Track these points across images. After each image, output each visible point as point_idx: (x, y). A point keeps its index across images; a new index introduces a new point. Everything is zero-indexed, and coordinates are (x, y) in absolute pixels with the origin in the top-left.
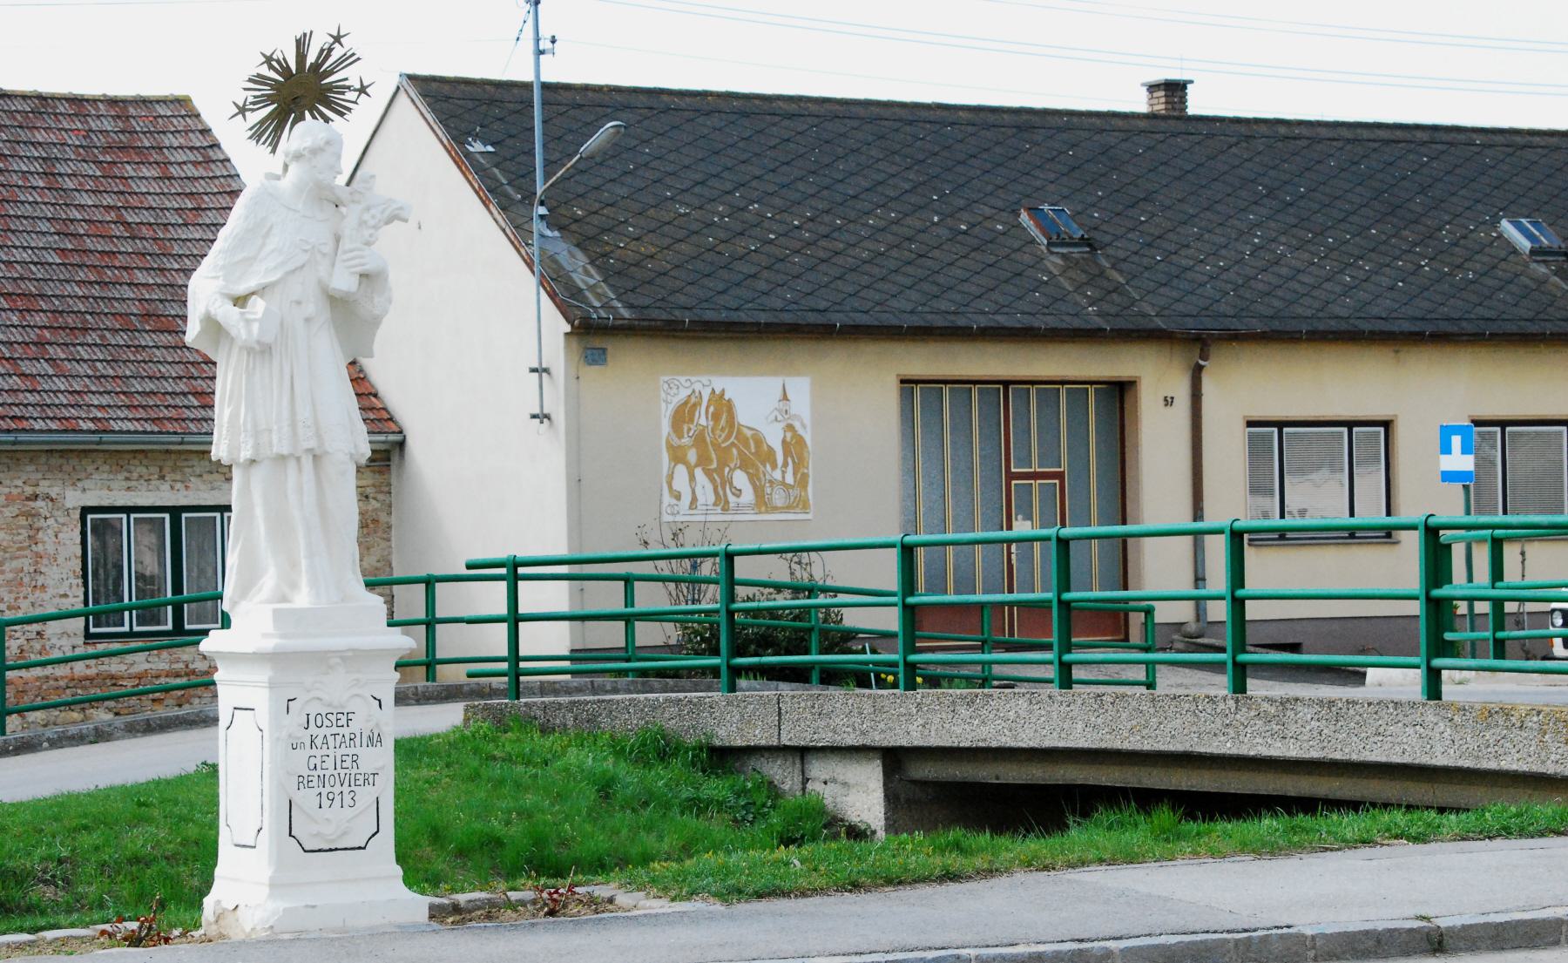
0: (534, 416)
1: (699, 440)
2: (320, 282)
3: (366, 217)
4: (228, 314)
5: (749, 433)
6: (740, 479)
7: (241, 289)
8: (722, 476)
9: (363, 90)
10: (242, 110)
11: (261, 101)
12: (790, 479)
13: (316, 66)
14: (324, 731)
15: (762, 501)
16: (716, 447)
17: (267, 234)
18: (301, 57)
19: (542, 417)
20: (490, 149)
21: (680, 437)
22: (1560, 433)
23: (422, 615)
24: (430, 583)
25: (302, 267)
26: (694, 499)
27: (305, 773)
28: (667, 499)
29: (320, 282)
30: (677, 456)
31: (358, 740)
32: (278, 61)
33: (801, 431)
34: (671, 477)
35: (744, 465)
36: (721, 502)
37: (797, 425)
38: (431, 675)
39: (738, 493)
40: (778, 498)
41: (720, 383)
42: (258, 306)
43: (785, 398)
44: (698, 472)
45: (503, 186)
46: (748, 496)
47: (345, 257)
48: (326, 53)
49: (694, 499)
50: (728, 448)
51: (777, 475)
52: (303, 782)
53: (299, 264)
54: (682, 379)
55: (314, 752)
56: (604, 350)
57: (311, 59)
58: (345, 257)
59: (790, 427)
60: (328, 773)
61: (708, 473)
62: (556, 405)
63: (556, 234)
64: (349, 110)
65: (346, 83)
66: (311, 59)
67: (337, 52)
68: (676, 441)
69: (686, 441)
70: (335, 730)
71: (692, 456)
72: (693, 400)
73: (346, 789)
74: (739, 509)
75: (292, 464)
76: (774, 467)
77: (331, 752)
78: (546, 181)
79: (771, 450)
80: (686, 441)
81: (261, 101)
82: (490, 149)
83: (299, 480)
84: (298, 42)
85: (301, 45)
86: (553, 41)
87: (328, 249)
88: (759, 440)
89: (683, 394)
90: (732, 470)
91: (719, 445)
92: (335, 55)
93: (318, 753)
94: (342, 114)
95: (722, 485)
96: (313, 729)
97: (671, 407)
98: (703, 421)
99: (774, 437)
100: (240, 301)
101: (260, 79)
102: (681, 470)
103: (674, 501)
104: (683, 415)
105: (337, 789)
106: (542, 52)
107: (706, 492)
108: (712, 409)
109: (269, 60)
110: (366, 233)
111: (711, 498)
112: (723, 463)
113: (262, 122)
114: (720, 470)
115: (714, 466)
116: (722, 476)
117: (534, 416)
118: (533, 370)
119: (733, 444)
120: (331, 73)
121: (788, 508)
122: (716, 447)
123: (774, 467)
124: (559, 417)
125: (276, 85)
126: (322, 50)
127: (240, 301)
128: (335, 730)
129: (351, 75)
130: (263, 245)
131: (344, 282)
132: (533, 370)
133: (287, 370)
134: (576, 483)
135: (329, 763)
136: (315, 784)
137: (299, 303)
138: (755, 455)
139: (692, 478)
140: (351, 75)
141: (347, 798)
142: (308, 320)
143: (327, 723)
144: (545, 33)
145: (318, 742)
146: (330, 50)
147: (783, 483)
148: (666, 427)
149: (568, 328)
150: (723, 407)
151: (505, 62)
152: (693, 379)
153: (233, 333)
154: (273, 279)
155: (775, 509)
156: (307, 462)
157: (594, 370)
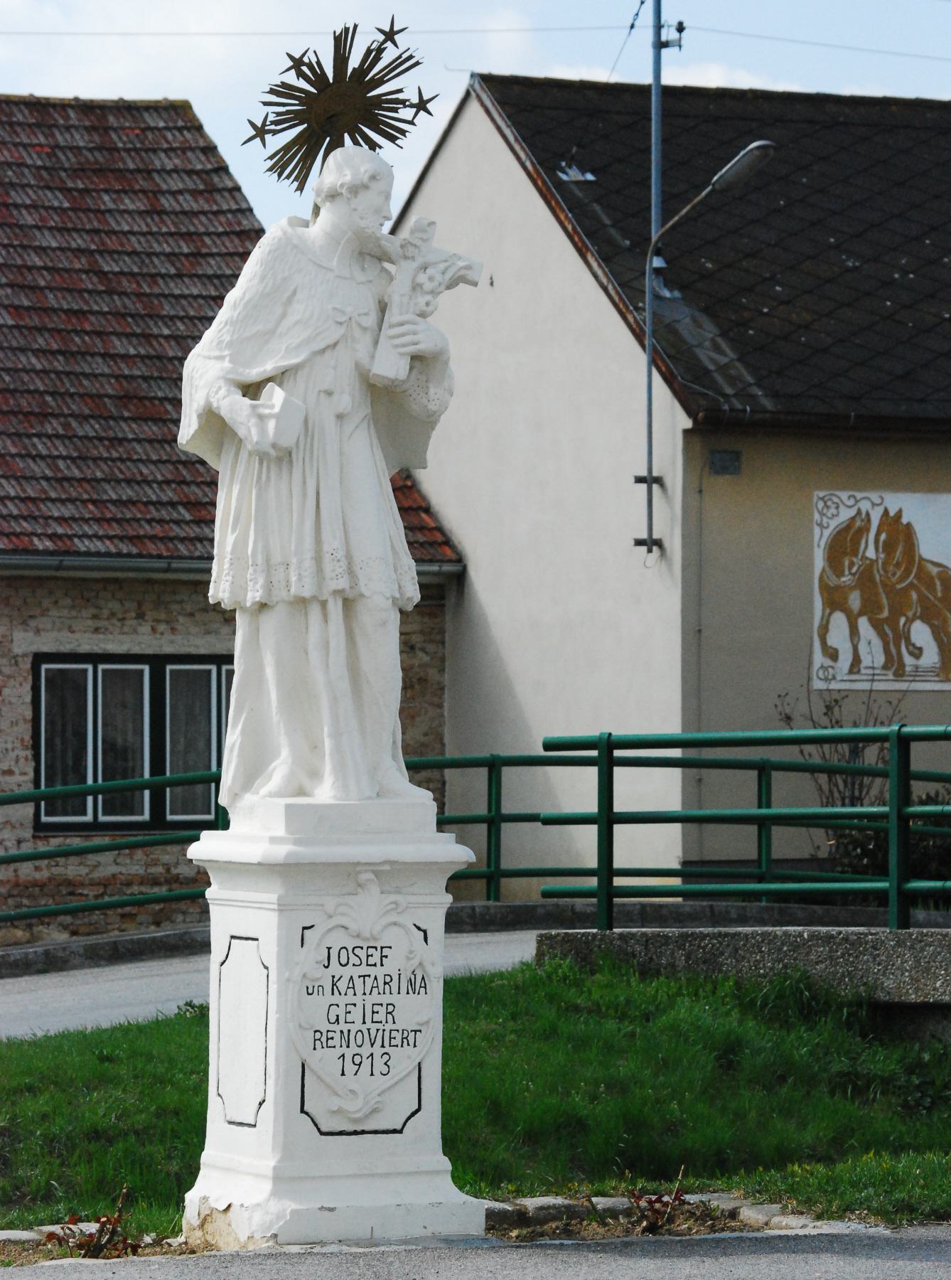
0: (639, 543)
1: (865, 579)
2: (357, 366)
3: (422, 278)
4: (234, 407)
7: (254, 373)
8: (895, 629)
9: (422, 106)
10: (260, 132)
11: (285, 121)
13: (361, 71)
14: (348, 972)
16: (890, 590)
17: (289, 301)
18: (341, 58)
19: (651, 543)
20: (590, 177)
21: (840, 574)
23: (482, 810)
24: (495, 766)
25: (335, 345)
26: (856, 660)
27: (324, 1027)
28: (819, 658)
29: (357, 366)
30: (834, 600)
31: (394, 985)
32: (310, 66)
34: (824, 629)
36: (893, 664)
38: (493, 890)
39: (917, 652)
41: (896, 501)
42: (275, 396)
44: (863, 623)
45: (603, 225)
48: (374, 54)
49: (856, 660)
50: (905, 590)
52: (321, 1039)
53: (331, 341)
54: (844, 495)
55: (336, 999)
56: (737, 455)
57: (354, 62)
60: (354, 1028)
61: (876, 625)
62: (670, 527)
63: (677, 294)
64: (403, 132)
65: (400, 96)
66: (354, 62)
67: (390, 54)
68: (833, 581)
70: (364, 970)
71: (855, 601)
72: (858, 523)
73: (377, 1050)
74: (917, 673)
75: (315, 612)
77: (358, 1000)
78: (664, 223)
81: (285, 121)
82: (590, 177)
83: (324, 632)
84: (337, 39)
85: (342, 42)
86: (680, 28)
87: (370, 321)
89: (846, 514)
90: (910, 621)
92: (390, 54)
93: (342, 1000)
94: (392, 139)
95: (895, 638)
96: (335, 968)
97: (827, 533)
98: (871, 553)
100: (252, 390)
101: (283, 90)
102: (839, 621)
103: (828, 662)
104: (844, 544)
105: (366, 1050)
106: (666, 45)
107: (873, 653)
108: (883, 536)
109: (297, 64)
110: (422, 300)
111: (880, 659)
112: (896, 612)
113: (287, 148)
114: (892, 621)
115: (886, 614)
116: (895, 629)
117: (639, 543)
118: (639, 480)
119: (911, 585)
120: (380, 82)
122: (890, 590)
124: (675, 544)
125: (306, 98)
126: (369, 52)
127: (252, 390)
128: (364, 970)
129: (408, 85)
130: (284, 315)
131: (391, 366)
132: (639, 480)
135: (356, 1014)
136: (336, 1042)
137: (329, 393)
139: (854, 631)
140: (408, 85)
142: (340, 417)
143: (354, 960)
144: (670, 18)
145: (342, 985)
146: (380, 50)
148: (819, 562)
149: (688, 424)
150: (899, 534)
152: (859, 495)
153: (241, 432)
156: (335, 608)
157: (722, 481)
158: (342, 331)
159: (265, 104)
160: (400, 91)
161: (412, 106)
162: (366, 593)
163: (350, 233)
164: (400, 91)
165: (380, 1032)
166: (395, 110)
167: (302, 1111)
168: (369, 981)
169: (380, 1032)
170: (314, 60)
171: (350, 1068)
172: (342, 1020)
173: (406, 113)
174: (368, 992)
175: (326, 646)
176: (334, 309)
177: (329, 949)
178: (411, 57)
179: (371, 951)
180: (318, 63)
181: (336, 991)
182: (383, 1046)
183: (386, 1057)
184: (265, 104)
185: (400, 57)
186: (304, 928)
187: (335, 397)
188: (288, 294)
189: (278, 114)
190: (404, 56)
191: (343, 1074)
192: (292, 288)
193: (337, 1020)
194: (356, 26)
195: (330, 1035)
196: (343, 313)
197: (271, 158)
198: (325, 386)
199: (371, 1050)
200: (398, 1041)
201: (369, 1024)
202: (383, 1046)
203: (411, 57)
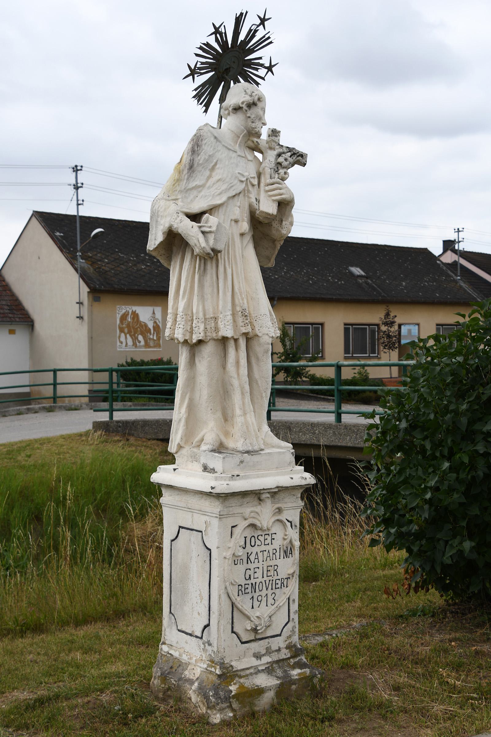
0: (77, 317)
1: (128, 326)
2: (250, 206)
3: (281, 159)
5: (143, 324)
6: (140, 338)
7: (195, 208)
8: (135, 336)
9: (270, 69)
10: (193, 72)
12: (155, 338)
13: (245, 42)
14: (256, 549)
15: (147, 345)
16: (133, 328)
17: (213, 169)
19: (81, 318)
20: (62, 234)
21: (123, 324)
22: (366, 328)
23: (52, 382)
24: (55, 371)
26: (127, 344)
28: (118, 344)
29: (250, 206)
30: (122, 330)
31: (278, 554)
32: (221, 34)
33: (158, 323)
34: (119, 337)
35: (142, 334)
36: (135, 345)
37: (157, 321)
38: (55, 402)
39: (140, 342)
40: (152, 344)
42: (211, 221)
43: (154, 313)
44: (128, 335)
45: (66, 246)
46: (143, 343)
47: (267, 188)
48: (252, 33)
49: (127, 344)
50: (137, 328)
51: (151, 337)
52: (242, 590)
54: (123, 307)
56: (99, 297)
57: (242, 37)
58: (267, 188)
59: (155, 322)
60: (258, 581)
61: (131, 336)
63: (84, 261)
65: (261, 61)
66: (242, 37)
68: (121, 326)
69: (124, 326)
70: (263, 548)
71: (126, 330)
73: (270, 592)
74: (140, 347)
75: (232, 343)
76: (150, 334)
79: (150, 329)
80: (124, 326)
82: (62, 234)
83: (236, 356)
86: (83, 201)
87: (255, 182)
88: (146, 325)
89: (124, 311)
90: (138, 335)
91: (134, 328)
95: (135, 339)
96: (249, 549)
97: (120, 315)
98: (129, 320)
99: (151, 325)
100: (195, 217)
102: (123, 335)
104: (124, 317)
106: (80, 204)
107: (130, 341)
110: (282, 171)
111: (132, 344)
112: (135, 333)
113: (203, 85)
114: (134, 335)
115: (133, 333)
116: (135, 336)
117: (77, 317)
118: (77, 303)
120: (252, 51)
121: (154, 347)
122: (133, 328)
123: (150, 334)
124: (86, 318)
126: (250, 30)
127: (195, 217)
128: (263, 548)
130: (210, 177)
131: (268, 207)
132: (77, 303)
133: (229, 271)
134: (91, 339)
135: (259, 574)
136: (249, 590)
137: (236, 221)
138: (144, 330)
139: (126, 338)
141: (270, 601)
142: (242, 235)
143: (258, 543)
144: (80, 198)
145: (252, 558)
146: (256, 31)
147: (153, 339)
148: (118, 322)
149: (88, 290)
150: (135, 315)
151: (68, 208)
153: (192, 242)
154: (219, 202)
155: (150, 347)
156: (242, 343)
157: (96, 304)
159: (197, 55)
160: (260, 58)
161: (265, 68)
162: (260, 334)
163: (246, 131)
164: (260, 58)
165: (271, 582)
166: (257, 69)
167: (233, 632)
169: (271, 582)
170: (223, 31)
171: (256, 604)
172: (252, 578)
174: (265, 560)
175: (238, 363)
176: (239, 173)
177: (245, 537)
178: (269, 38)
179: (267, 537)
180: (225, 33)
181: (249, 561)
183: (274, 595)
184: (197, 55)
185: (264, 37)
186: (233, 527)
187: (240, 223)
188: (213, 164)
189: (202, 63)
190: (267, 36)
191: (253, 608)
192: (215, 161)
193: (250, 578)
194: (247, 12)
195: (247, 586)
196: (243, 175)
197: (196, 90)
198: (233, 218)
199: (267, 592)
200: (279, 586)
201: (265, 578)
202: (272, 589)
203: (269, 38)
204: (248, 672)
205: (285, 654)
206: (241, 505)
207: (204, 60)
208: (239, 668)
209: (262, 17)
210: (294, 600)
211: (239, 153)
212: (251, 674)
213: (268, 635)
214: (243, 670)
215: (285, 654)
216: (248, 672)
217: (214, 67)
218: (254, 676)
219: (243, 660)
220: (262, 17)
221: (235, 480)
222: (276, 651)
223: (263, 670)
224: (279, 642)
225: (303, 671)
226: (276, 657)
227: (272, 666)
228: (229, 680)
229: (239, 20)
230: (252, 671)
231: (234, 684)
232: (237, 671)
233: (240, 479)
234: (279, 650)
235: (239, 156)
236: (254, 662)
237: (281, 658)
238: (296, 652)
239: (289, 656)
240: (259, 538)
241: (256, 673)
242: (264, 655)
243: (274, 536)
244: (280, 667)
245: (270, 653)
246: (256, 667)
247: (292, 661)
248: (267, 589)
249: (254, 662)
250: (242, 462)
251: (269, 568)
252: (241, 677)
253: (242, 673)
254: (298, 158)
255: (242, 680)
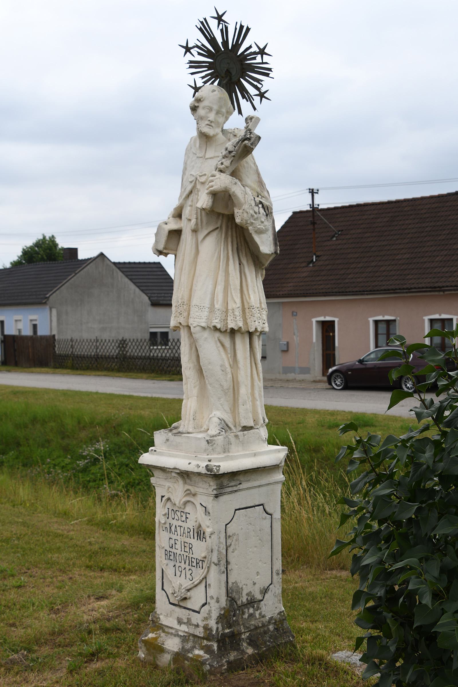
9: (262, 52)
27: (169, 549)
48: (225, 32)
57: (219, 40)
66: (219, 40)
70: (180, 523)
84: (200, 29)
94: (267, 75)
120: (237, 45)
128: (180, 523)
158: (193, 184)
159: (192, 74)
164: (250, 47)
168: (182, 529)
169: (188, 558)
170: (199, 44)
171: (178, 573)
173: (259, 59)
178: (242, 27)
180: (203, 45)
182: (189, 565)
183: (191, 572)
184: (192, 74)
185: (236, 29)
189: (203, 78)
200: (194, 564)
202: (189, 565)
204: (171, 631)
205: (200, 632)
206: (166, 479)
207: (203, 74)
208: (163, 623)
209: (216, 16)
210: (209, 585)
211: (198, 155)
212: (172, 634)
213: (189, 607)
214: (167, 627)
215: (200, 632)
216: (171, 631)
217: (214, 75)
218: (173, 636)
219: (169, 618)
220: (216, 16)
221: (154, 454)
222: (195, 625)
223: (181, 636)
224: (196, 619)
225: (205, 655)
226: (192, 630)
227: (189, 636)
228: (156, 628)
229: (204, 29)
230: (173, 631)
231: (156, 634)
232: (162, 624)
233: (157, 455)
234: (197, 626)
235: (198, 157)
236: (176, 626)
237: (196, 634)
238: (208, 636)
239: (202, 635)
240: (177, 512)
241: (175, 635)
242: (184, 623)
243: (188, 515)
244: (193, 642)
245: (190, 625)
246: (177, 630)
247: (205, 642)
248: (185, 563)
249: (176, 626)
250: (167, 440)
251: (186, 544)
252: (164, 631)
253: (166, 630)
254: (244, 143)
255: (163, 634)
